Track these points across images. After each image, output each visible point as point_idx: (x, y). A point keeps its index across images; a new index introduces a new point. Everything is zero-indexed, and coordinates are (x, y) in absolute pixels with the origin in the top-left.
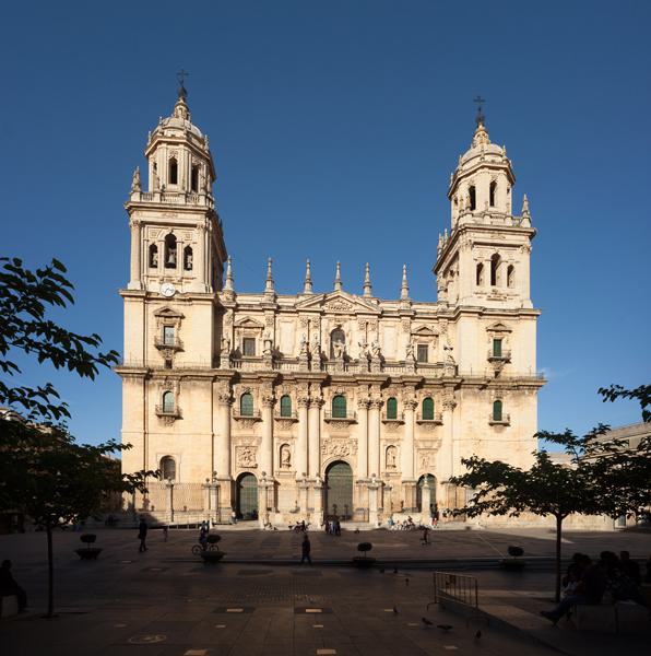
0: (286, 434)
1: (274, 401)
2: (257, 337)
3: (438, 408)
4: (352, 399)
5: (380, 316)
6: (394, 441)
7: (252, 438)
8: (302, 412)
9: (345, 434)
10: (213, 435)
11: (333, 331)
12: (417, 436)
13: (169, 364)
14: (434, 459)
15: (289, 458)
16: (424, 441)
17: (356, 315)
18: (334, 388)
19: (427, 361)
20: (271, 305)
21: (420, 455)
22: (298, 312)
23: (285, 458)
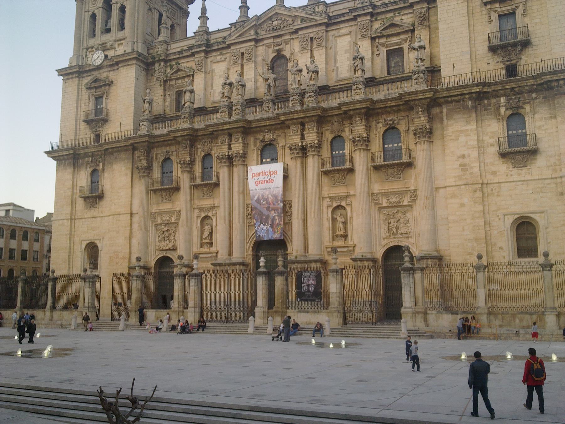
0: (207, 203)
1: (192, 163)
5: (327, 25)
6: (342, 198)
7: (171, 213)
8: (223, 173)
10: (132, 214)
11: (274, 60)
12: (377, 188)
15: (211, 233)
16: (386, 194)
17: (296, 31)
18: (260, 137)
20: (199, 46)
21: (383, 217)
22: (229, 46)
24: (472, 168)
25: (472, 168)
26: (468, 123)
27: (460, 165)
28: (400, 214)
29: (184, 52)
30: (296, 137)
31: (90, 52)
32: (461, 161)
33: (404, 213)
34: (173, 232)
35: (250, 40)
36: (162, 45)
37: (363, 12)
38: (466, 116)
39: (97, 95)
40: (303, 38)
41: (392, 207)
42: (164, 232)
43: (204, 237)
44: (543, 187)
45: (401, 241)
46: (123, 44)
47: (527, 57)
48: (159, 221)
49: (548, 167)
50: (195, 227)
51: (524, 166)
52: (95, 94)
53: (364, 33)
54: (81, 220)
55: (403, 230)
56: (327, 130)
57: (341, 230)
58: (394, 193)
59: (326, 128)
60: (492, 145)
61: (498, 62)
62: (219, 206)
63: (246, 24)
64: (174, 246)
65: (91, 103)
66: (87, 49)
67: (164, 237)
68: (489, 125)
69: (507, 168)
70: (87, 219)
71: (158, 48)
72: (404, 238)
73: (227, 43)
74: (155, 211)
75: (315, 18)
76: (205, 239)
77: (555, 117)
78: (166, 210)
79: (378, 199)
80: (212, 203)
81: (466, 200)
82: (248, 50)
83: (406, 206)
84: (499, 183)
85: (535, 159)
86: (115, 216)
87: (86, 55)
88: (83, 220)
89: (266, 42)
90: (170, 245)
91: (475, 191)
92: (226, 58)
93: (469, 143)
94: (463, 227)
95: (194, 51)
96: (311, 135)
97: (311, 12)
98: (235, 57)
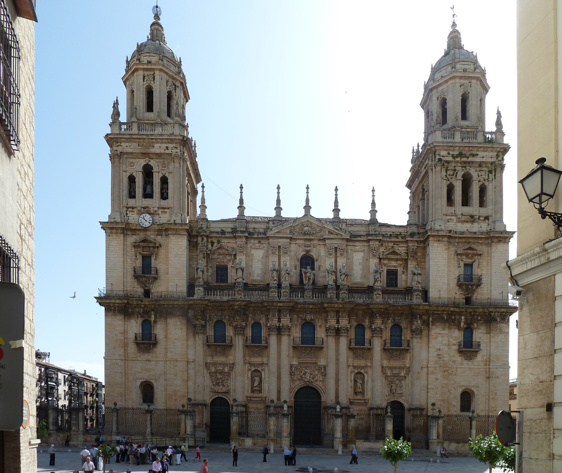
2: (230, 265)
3: (406, 335)
4: (320, 326)
7: (225, 364)
9: (314, 360)
12: (385, 363)
13: (147, 293)
14: (401, 387)
16: (391, 368)
19: (396, 285)
20: (243, 232)
22: (268, 238)
23: (256, 384)
24: (444, 357)
25: (444, 357)
26: (444, 329)
27: (437, 355)
28: (397, 381)
29: (226, 233)
30: (333, 321)
31: (129, 211)
32: (438, 352)
33: (400, 381)
34: (226, 380)
35: (286, 238)
36: (204, 222)
37: (375, 238)
38: (443, 325)
40: (330, 246)
41: (394, 376)
42: (218, 378)
43: (255, 385)
44: (479, 373)
45: (398, 398)
46: (166, 212)
47: (477, 294)
48: (213, 370)
49: (483, 361)
50: (246, 377)
51: (471, 360)
53: (375, 254)
54: (134, 362)
55: (399, 391)
56: (353, 319)
57: (360, 389)
58: (396, 368)
59: (353, 318)
60: (455, 345)
61: (461, 294)
62: (267, 364)
63: (285, 224)
64: (227, 390)
65: (138, 260)
66: (128, 208)
67: (219, 383)
68: (454, 332)
69: (462, 359)
70: (140, 362)
71: (202, 225)
72: (400, 396)
73: (268, 235)
74: (210, 362)
75: (341, 233)
76: (255, 387)
77: (490, 333)
78: (220, 362)
79: (386, 371)
80: (262, 360)
81: (439, 376)
82: (285, 245)
83: (402, 376)
84: (457, 368)
85: (476, 356)
86: (172, 362)
87: (127, 214)
88: (137, 362)
90: (225, 389)
91: (445, 372)
93: (443, 342)
94: (436, 392)
95: (237, 235)
96: (344, 321)
97: (338, 228)
98: (274, 248)
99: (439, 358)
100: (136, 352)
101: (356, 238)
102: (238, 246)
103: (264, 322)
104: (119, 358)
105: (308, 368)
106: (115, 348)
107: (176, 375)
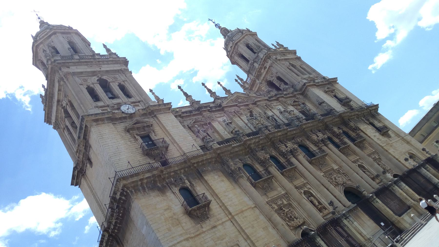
7: (281, 197)
39: (142, 134)
52: (139, 133)
70: (206, 233)
73: (223, 106)
76: (318, 205)
78: (276, 196)
88: (203, 235)
89: (241, 107)
92: (224, 115)
95: (202, 110)
99: (380, 140)
100: (193, 224)
101: (270, 98)
102: (208, 117)
103: (276, 153)
104: (182, 238)
105: (333, 174)
106: (169, 230)
107: (253, 227)
